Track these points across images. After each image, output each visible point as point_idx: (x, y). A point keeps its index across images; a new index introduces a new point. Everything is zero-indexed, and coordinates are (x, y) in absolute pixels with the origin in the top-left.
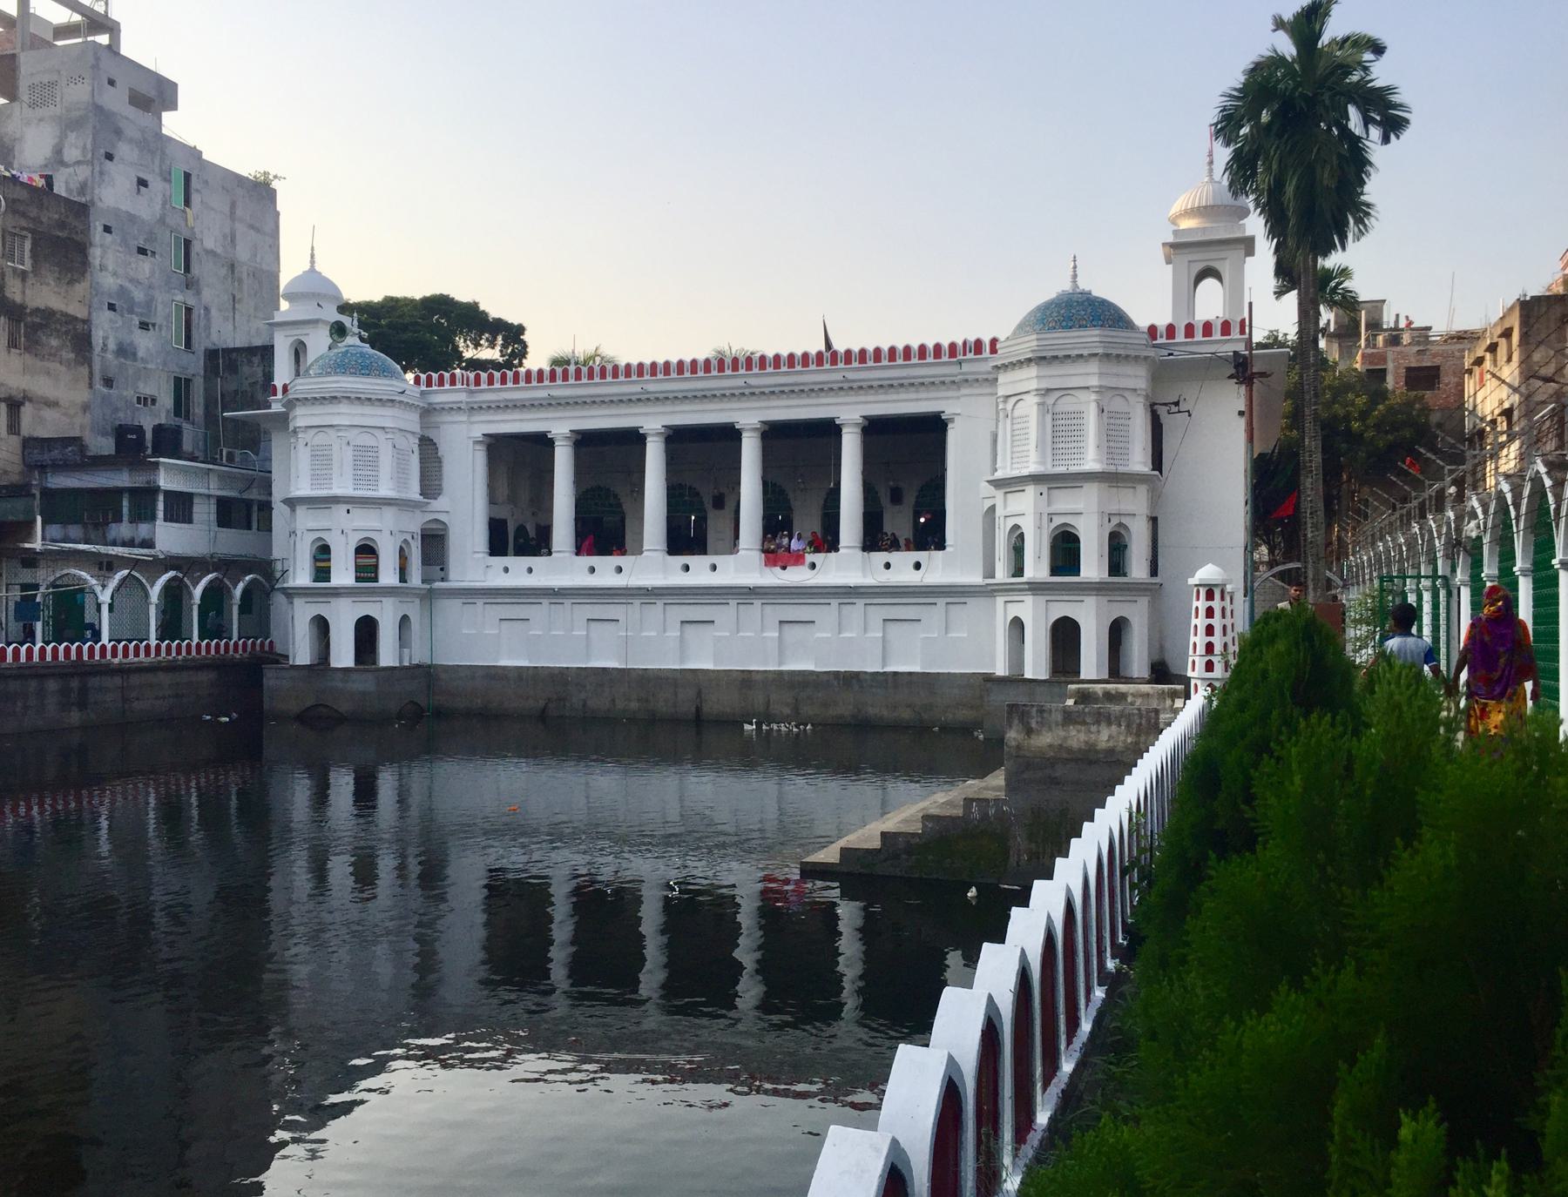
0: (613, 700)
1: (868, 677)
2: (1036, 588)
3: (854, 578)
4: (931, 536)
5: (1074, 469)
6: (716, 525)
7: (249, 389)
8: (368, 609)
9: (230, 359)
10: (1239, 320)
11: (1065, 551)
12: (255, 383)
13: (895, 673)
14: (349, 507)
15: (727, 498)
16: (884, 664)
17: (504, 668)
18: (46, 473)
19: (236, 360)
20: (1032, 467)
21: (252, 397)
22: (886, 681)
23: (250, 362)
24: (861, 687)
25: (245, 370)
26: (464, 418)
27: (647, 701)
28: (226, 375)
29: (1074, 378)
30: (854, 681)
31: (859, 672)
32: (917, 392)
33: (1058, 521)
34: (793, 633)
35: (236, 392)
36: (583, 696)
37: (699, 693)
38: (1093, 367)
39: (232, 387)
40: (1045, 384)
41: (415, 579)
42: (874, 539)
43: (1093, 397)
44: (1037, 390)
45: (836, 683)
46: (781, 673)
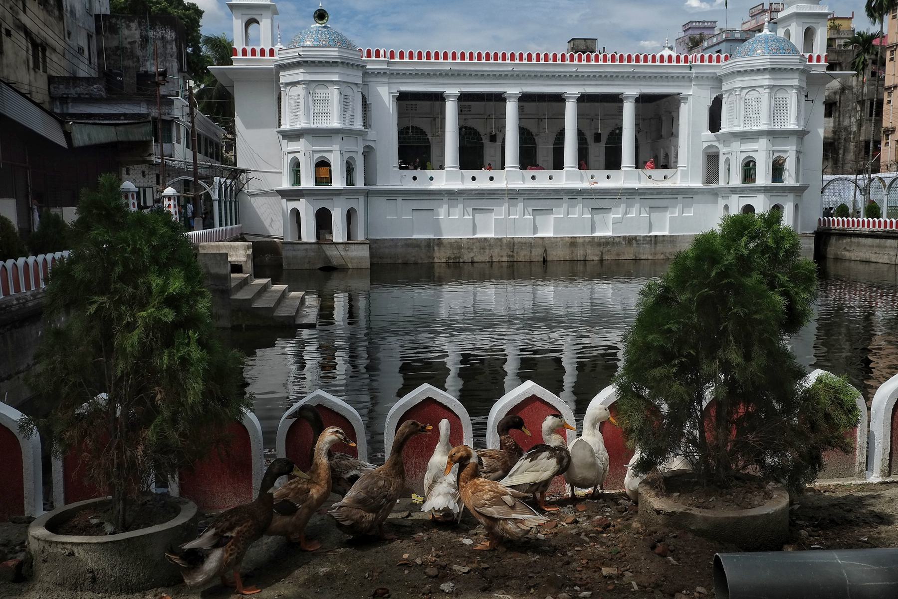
0: (492, 257)
1: (641, 239)
2: (766, 190)
3: (635, 185)
4: (665, 162)
5: (784, 128)
6: (490, 151)
7: (128, 46)
8: (352, 204)
9: (110, 23)
10: (824, 55)
11: (777, 170)
12: (135, 42)
13: (656, 236)
14: (343, 136)
15: (498, 137)
16: (650, 231)
17: (415, 239)
18: (67, 103)
19: (116, 24)
20: (763, 127)
21: (132, 52)
22: (651, 240)
23: (128, 27)
24: (638, 244)
25: (126, 32)
26: (387, 80)
27: (512, 256)
28: (108, 34)
29: (786, 81)
30: (634, 241)
31: (636, 237)
32: (674, 81)
33: (776, 155)
34: (598, 217)
35: (117, 48)
36: (472, 255)
37: (545, 251)
38: (796, 75)
39: (115, 43)
40: (773, 83)
41: (360, 184)
42: (528, 160)
43: (794, 91)
44: (769, 85)
45: (624, 243)
46: (593, 238)
